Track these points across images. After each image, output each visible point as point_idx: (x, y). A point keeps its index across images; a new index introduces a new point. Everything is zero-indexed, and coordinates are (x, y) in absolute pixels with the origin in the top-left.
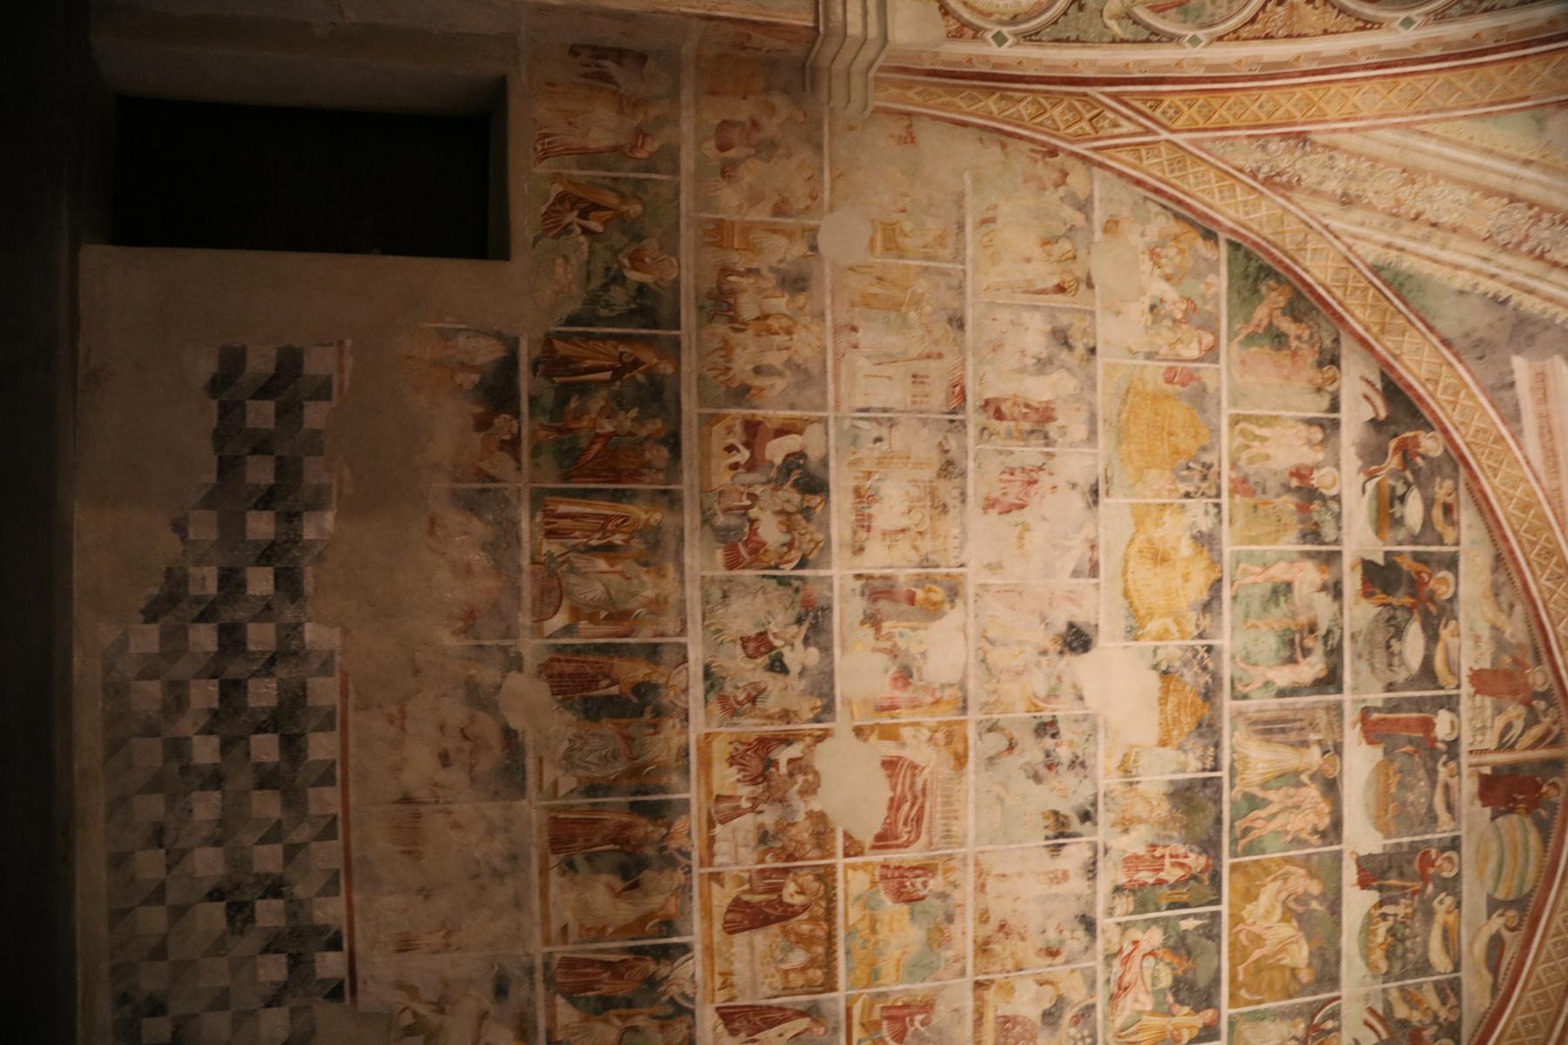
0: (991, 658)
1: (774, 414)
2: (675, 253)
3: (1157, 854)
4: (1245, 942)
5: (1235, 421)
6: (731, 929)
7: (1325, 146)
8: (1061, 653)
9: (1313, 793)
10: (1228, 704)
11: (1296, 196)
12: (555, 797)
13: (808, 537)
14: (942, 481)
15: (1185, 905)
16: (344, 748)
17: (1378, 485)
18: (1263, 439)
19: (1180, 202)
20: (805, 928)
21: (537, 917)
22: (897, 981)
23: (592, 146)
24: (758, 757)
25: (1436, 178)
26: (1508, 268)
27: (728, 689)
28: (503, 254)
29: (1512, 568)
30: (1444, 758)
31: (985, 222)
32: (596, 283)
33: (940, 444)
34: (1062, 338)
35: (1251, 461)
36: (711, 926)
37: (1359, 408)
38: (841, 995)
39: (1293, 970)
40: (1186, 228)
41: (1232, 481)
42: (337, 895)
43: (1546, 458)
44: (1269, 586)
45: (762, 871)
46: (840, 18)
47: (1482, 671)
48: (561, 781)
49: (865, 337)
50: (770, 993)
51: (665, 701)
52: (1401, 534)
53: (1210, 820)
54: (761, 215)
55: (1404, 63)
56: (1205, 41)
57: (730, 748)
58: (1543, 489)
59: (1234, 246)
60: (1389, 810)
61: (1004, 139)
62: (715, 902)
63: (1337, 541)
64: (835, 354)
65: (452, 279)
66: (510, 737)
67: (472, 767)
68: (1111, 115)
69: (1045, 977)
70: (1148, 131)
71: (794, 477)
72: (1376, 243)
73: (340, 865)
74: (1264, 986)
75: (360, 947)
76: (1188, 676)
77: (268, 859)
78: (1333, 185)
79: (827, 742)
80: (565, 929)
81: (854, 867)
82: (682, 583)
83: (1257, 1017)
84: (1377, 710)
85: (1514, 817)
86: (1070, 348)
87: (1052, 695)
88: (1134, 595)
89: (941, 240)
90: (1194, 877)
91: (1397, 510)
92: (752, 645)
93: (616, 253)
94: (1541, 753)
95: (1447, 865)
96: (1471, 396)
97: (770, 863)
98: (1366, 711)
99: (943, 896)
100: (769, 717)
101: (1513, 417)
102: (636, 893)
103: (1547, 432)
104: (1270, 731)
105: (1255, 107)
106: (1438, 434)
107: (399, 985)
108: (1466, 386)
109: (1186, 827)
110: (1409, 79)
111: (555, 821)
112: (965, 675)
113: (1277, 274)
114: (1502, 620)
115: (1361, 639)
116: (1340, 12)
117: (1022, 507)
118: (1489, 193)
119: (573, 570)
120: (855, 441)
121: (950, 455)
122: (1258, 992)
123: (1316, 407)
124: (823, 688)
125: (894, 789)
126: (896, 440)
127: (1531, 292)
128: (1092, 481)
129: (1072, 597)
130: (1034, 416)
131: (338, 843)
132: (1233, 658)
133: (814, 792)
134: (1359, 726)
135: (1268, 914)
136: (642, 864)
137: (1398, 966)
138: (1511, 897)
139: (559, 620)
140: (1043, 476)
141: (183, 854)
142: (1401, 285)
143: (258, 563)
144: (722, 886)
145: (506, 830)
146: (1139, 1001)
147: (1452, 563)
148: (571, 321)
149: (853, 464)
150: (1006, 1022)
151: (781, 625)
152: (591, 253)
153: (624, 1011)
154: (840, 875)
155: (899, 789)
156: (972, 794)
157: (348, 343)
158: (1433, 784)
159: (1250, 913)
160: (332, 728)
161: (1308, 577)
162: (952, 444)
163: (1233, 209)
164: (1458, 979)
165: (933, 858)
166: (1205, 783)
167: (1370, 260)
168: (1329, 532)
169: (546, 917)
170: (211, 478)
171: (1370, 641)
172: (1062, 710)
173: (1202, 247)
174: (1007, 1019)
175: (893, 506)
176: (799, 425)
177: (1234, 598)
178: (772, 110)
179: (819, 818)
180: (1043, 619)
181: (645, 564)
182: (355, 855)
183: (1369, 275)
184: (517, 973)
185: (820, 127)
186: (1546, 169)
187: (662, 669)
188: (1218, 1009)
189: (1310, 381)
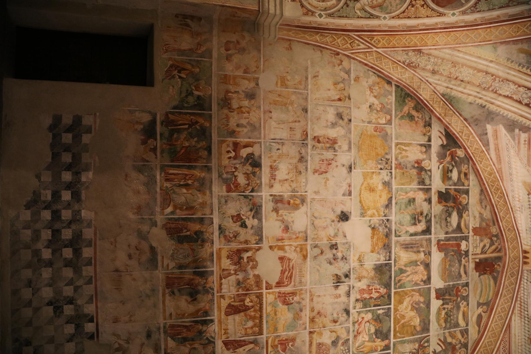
0: (315, 223)
1: (243, 140)
2: (210, 85)
3: (370, 288)
4: (399, 318)
5: (397, 144)
6: (227, 314)
7: (427, 54)
8: (339, 221)
9: (421, 268)
10: (394, 239)
11: (418, 70)
12: (168, 270)
13: (254, 182)
14: (300, 163)
15: (379, 305)
16: (95, 253)
17: (443, 166)
18: (406, 151)
19: (380, 72)
20: (253, 314)
21: (162, 310)
22: (283, 332)
23: (183, 48)
24: (237, 256)
25: (463, 65)
26: (485, 96)
27: (227, 233)
28: (151, 84)
29: (486, 194)
30: (464, 256)
31: (315, 77)
32: (184, 95)
33: (299, 151)
34: (340, 116)
35: (402, 158)
36: (221, 313)
37: (437, 142)
38: (264, 336)
39: (414, 326)
40: (382, 80)
41: (395, 164)
42: (92, 303)
43: (497, 158)
44: (407, 199)
45: (238, 295)
46: (267, 7)
47: (476, 227)
48: (170, 264)
49: (274, 115)
50: (241, 336)
51: (205, 237)
52: (451, 182)
53: (388, 277)
54: (240, 73)
55: (453, 28)
56: (388, 18)
57: (227, 253)
58: (496, 168)
59: (397, 86)
60: (446, 273)
61: (322, 49)
62: (222, 305)
63: (430, 185)
64: (264, 120)
65: (134, 92)
66: (152, 249)
67: (139, 259)
68: (357, 42)
69: (333, 330)
70: (369, 48)
71: (250, 162)
72: (443, 86)
73: (94, 293)
74: (405, 332)
75: (100, 321)
76: (381, 229)
77: (68, 291)
78: (429, 67)
79: (260, 251)
80: (171, 314)
81: (269, 293)
82: (212, 197)
83: (403, 342)
84: (442, 240)
85: (486, 276)
86: (343, 119)
87: (336, 235)
88: (363, 202)
89: (300, 83)
90: (382, 296)
91: (449, 174)
92: (235, 218)
93: (190, 85)
94: (495, 255)
95: (464, 291)
96: (474, 137)
97: (241, 292)
98: (439, 241)
99: (299, 303)
100: (241, 243)
101: (487, 144)
102: (195, 302)
103: (497, 149)
104: (407, 248)
105: (404, 41)
106: (463, 150)
107: (114, 334)
108: (472, 134)
109: (380, 279)
110: (454, 33)
111: (168, 278)
112: (307, 229)
113: (411, 96)
114: (483, 211)
115: (437, 217)
116: (432, 10)
117: (326, 172)
118: (479, 71)
119: (174, 192)
120: (270, 150)
121: (302, 155)
122: (403, 334)
123: (423, 140)
124: (259, 232)
125: (283, 267)
126: (285, 149)
127: (492, 103)
128: (350, 164)
129: (342, 203)
130: (331, 142)
131: (93, 286)
132: (395, 223)
133: (256, 268)
134: (436, 246)
135: (406, 308)
136: (197, 292)
137: (448, 325)
138: (485, 302)
139: (170, 209)
140: (333, 162)
141: (38, 289)
142: (451, 100)
143: (65, 189)
144: (225, 300)
145: (151, 281)
146: (364, 337)
147: (467, 192)
148: (175, 108)
149: (270, 157)
150: (320, 345)
151: (245, 211)
152: (182, 85)
153: (191, 342)
154: (264, 296)
155: (284, 267)
156: (309, 268)
157: (98, 114)
158: (460, 265)
159: (400, 308)
160: (91, 246)
161: (420, 196)
162: (303, 151)
163: (397, 74)
164: (468, 329)
165: (296, 290)
166: (386, 265)
167: (441, 92)
168: (427, 182)
169: (164, 310)
170: (50, 160)
171: (440, 218)
172: (339, 240)
173: (387, 87)
174: (320, 344)
175: (283, 172)
176: (252, 144)
177: (396, 203)
178: (243, 37)
179: (257, 277)
180: (333, 210)
181: (199, 191)
182: (99, 289)
183: (441, 97)
185: (260, 44)
186: (498, 64)
187: (205, 226)
188: (390, 340)
189: (422, 132)
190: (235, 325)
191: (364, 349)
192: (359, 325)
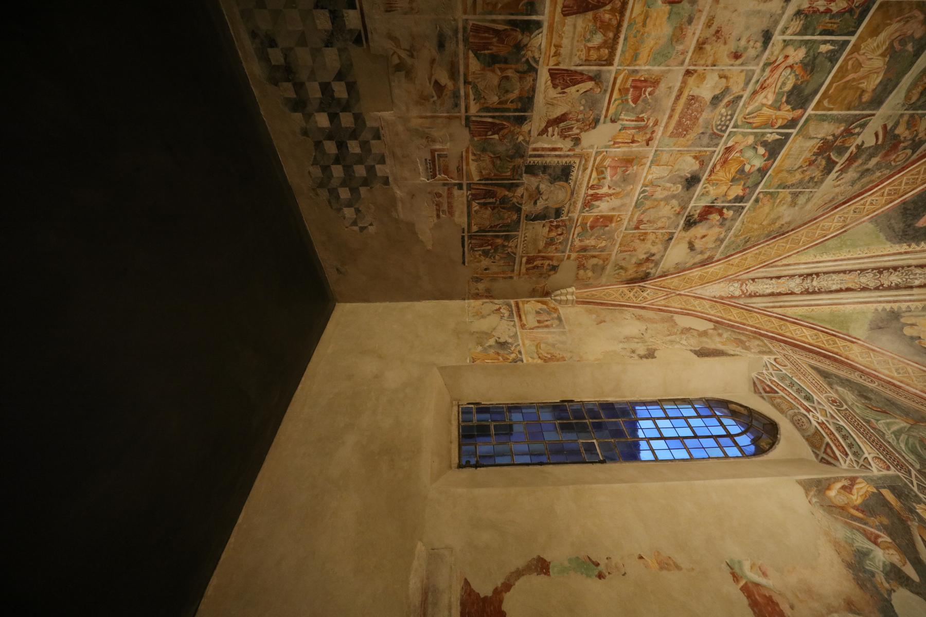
22: (646, 64)
36: (555, 9)
50: (578, 62)
75: (365, 7)
83: (823, 118)
107: (391, 37)
122: (834, 104)
146: (769, 97)
150: (693, 98)
153: (502, 66)
184: (450, 33)
190: (573, 38)
191: (755, 120)
192: (772, 71)
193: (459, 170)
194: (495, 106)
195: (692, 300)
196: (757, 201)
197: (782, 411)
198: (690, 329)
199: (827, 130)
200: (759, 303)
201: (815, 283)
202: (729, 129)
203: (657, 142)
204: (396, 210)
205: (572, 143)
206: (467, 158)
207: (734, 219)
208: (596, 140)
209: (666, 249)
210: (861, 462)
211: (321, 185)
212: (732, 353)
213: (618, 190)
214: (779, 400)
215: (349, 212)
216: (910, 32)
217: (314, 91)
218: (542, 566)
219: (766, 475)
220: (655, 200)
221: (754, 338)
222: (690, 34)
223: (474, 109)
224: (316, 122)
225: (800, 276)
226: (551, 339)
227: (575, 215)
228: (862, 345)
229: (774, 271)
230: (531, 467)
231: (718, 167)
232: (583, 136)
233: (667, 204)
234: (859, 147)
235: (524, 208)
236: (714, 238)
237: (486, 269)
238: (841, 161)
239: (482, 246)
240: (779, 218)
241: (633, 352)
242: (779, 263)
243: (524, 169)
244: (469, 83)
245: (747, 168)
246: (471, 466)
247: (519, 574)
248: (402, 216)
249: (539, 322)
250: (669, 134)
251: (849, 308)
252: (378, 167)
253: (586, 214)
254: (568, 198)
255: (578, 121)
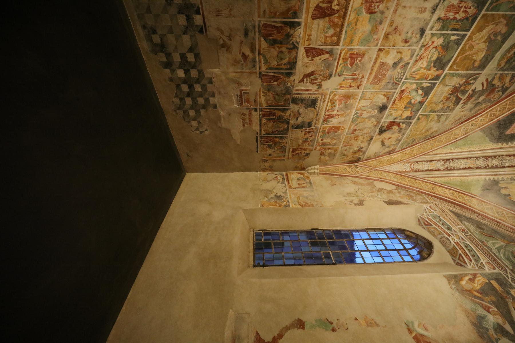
3: (461, 5)
6: (314, 17)
21: (257, 6)
22: (357, 45)
36: (308, 16)
50: (320, 44)
62: (311, 6)
75: (205, 13)
80: (265, 11)
83: (454, 75)
99: (382, 13)
107: (219, 29)
122: (459, 67)
146: (423, 63)
150: (383, 64)
153: (279, 45)
169: (259, 6)
184: (251, 28)
190: (318, 31)
191: (416, 76)
192: (425, 50)
193: (255, 101)
194: (275, 67)
195: (383, 173)
196: (418, 119)
197: (434, 236)
198: (383, 189)
199: (456, 81)
200: (421, 175)
201: (451, 164)
202: (403, 80)
203: (363, 87)
204: (220, 122)
205: (317, 87)
206: (260, 94)
207: (406, 129)
208: (330, 85)
209: (369, 145)
210: (479, 265)
211: (179, 108)
212: (406, 203)
213: (342, 112)
214: (433, 230)
215: (194, 123)
216: (499, 30)
217: (177, 58)
218: (300, 324)
219: (426, 272)
220: (363, 118)
221: (419, 194)
222: (380, 30)
223: (264, 68)
224: (177, 74)
225: (443, 160)
226: (305, 194)
227: (319, 126)
228: (478, 199)
229: (429, 158)
230: (294, 267)
231: (397, 101)
232: (323, 83)
233: (370, 120)
234: (473, 91)
235: (291, 122)
236: (395, 139)
237: (270, 155)
238: (464, 98)
239: (267, 142)
240: (431, 128)
241: (351, 202)
242: (431, 153)
243: (291, 100)
244: (261, 54)
245: (413, 101)
246: (261, 266)
247: (287, 329)
248: (223, 125)
249: (299, 184)
250: (370, 83)
251: (471, 178)
252: (211, 99)
253: (325, 125)
254: (315, 117)
255: (320, 75)
